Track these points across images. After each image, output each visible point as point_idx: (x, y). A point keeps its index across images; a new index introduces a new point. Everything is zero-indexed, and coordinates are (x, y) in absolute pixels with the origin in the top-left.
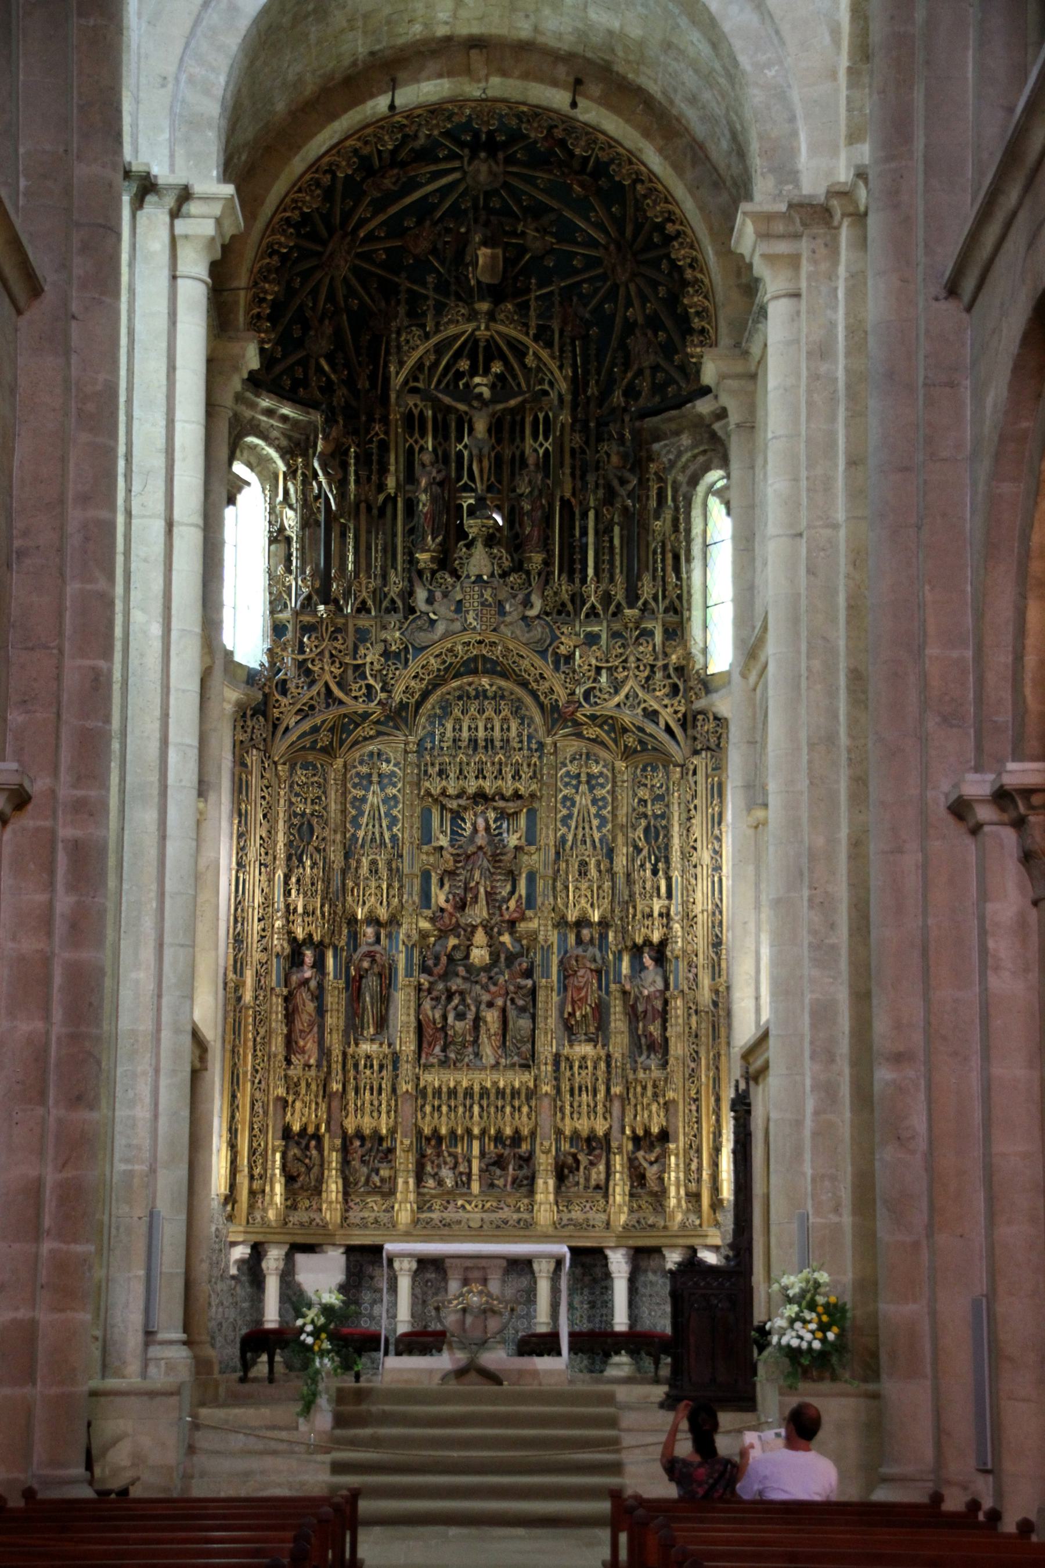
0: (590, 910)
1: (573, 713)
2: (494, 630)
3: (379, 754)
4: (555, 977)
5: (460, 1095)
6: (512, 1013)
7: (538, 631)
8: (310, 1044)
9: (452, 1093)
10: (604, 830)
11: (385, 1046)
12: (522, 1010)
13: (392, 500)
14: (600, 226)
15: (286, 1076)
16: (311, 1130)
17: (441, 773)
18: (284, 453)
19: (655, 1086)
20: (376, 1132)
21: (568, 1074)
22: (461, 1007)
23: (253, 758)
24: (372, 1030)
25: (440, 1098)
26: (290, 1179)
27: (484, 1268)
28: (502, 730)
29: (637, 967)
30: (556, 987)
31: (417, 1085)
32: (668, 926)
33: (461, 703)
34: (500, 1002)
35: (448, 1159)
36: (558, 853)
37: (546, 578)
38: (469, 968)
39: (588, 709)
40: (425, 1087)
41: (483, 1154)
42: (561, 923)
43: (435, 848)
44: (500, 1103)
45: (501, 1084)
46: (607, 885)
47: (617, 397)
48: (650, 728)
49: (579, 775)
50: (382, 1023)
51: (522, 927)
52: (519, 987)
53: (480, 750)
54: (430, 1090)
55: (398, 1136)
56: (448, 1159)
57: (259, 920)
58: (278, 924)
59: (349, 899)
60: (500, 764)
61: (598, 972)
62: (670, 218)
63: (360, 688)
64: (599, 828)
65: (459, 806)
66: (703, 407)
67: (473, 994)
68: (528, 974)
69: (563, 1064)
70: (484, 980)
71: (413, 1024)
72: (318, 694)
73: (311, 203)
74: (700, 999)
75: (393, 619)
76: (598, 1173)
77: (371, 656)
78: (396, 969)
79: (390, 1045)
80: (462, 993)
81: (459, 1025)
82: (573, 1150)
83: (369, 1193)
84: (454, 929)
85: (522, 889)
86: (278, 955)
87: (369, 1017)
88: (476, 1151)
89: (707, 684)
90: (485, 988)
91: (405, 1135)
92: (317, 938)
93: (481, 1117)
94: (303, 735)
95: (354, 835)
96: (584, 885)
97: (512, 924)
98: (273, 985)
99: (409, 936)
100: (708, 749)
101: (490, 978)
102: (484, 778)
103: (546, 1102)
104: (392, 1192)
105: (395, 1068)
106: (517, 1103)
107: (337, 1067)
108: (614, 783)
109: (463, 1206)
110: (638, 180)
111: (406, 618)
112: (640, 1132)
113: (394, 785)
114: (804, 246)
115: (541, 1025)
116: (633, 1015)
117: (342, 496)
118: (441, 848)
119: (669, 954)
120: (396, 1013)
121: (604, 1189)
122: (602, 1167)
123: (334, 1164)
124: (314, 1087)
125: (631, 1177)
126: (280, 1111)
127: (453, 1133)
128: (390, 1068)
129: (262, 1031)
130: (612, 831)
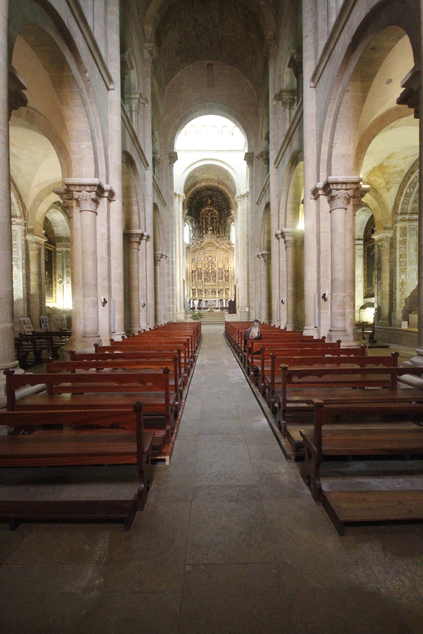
7: (215, 239)
8: (194, 281)
13: (201, 226)
14: (221, 198)
18: (190, 222)
23: (188, 252)
26: (193, 293)
29: (226, 272)
37: (216, 234)
39: (220, 247)
42: (218, 268)
47: (223, 215)
48: (227, 249)
50: (201, 278)
51: (214, 269)
62: (228, 197)
66: (232, 216)
68: (215, 273)
73: (192, 196)
75: (201, 238)
76: (222, 292)
77: (199, 242)
87: (200, 278)
89: (232, 245)
104: (202, 295)
110: (225, 193)
114: (242, 199)
116: (225, 277)
117: (196, 226)
121: (223, 294)
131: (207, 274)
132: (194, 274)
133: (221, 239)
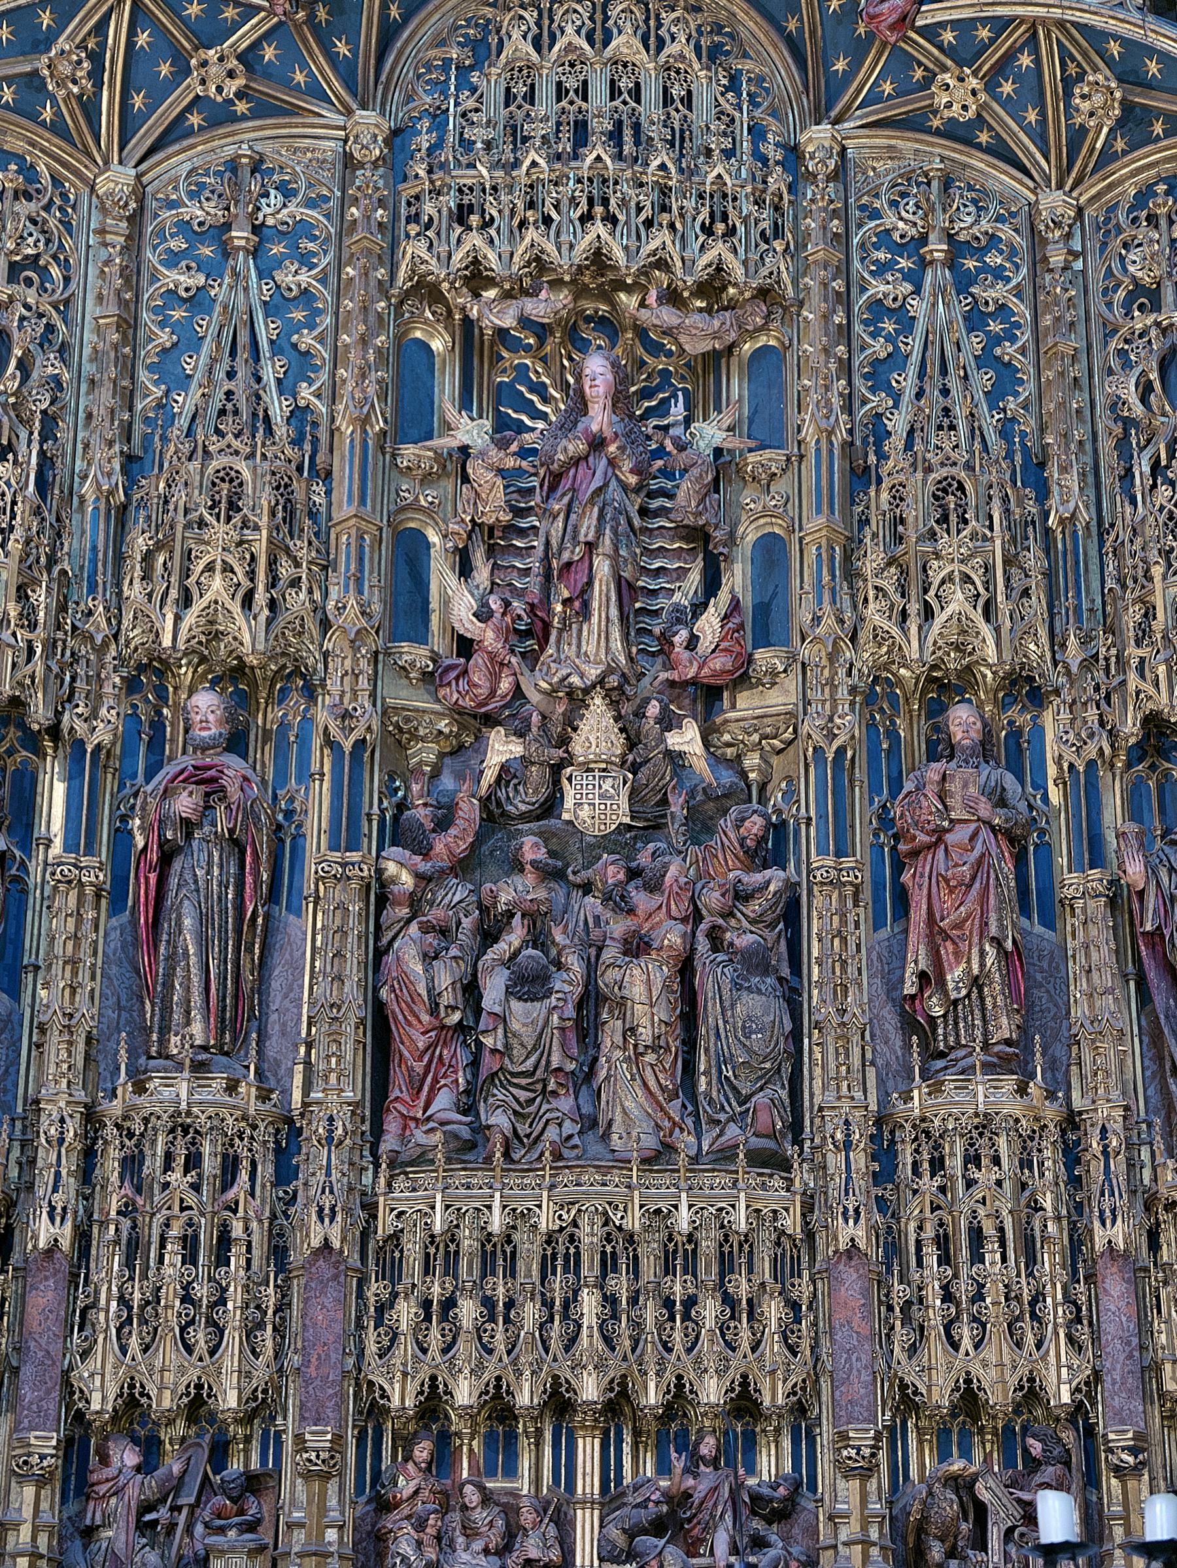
0: (986, 630)
1: (903, 21)
3: (256, 167)
5: (529, 1268)
17: (461, 215)
22: (530, 951)
25: (451, 1268)
28: (667, 100)
30: (866, 895)
34: (672, 936)
40: (395, 1237)
43: (440, 457)
45: (683, 1220)
49: (923, 239)
52: (742, 896)
56: (480, 1516)
59: (134, 591)
60: (665, 191)
64: (994, 397)
65: (525, 322)
70: (614, 874)
71: (355, 1006)
78: (298, 837)
88: (588, 1482)
90: (619, 902)
93: (607, 1340)
95: (160, 406)
101: (634, 874)
102: (611, 219)
105: (285, 1173)
106: (742, 1288)
108: (1039, 262)
113: (306, 261)
118: (464, 450)
120: (294, 985)
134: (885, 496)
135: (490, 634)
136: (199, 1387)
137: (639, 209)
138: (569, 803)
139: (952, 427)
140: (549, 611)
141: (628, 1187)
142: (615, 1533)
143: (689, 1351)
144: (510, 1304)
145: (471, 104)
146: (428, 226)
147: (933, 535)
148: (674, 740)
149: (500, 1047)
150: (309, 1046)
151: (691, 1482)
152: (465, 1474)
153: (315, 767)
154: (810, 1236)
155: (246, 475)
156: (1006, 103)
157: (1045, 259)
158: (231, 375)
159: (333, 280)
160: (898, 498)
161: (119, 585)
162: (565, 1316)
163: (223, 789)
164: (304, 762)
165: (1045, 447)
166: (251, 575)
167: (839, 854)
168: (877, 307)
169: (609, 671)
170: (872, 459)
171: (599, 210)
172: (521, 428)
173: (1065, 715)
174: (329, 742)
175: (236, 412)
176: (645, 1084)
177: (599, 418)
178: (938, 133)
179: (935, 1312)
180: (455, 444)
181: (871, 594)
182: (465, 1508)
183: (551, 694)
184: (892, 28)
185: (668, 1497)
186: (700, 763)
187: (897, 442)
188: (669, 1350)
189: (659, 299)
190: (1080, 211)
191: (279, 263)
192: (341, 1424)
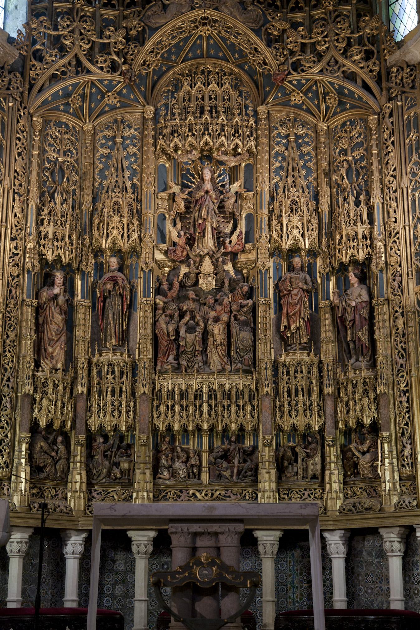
2: (216, 9)
4: (272, 296)
5: (191, 397)
6: (235, 327)
9: (184, 395)
10: (311, 179)
11: (126, 356)
12: (245, 324)
15: (33, 375)
16: (56, 426)
19: (365, 383)
20: (116, 429)
21: (286, 377)
22: (191, 322)
24: (113, 341)
25: (173, 398)
27: (216, 534)
28: (224, 100)
30: (272, 306)
31: (154, 389)
32: (372, 246)
33: (189, 78)
34: (225, 317)
35: (181, 454)
36: (272, 198)
38: (199, 293)
39: (295, 76)
40: (160, 390)
41: (211, 450)
44: (226, 403)
45: (227, 387)
46: (315, 221)
49: (288, 135)
51: (242, 258)
52: (242, 307)
53: (206, 113)
54: (164, 393)
55: (137, 433)
56: (181, 454)
57: (12, 239)
58: (30, 245)
59: (95, 233)
61: (308, 292)
63: (105, 61)
64: (306, 177)
67: (202, 313)
69: (280, 370)
70: (211, 301)
72: (69, 64)
74: (405, 302)
78: (136, 292)
79: (129, 357)
80: (192, 312)
81: (190, 337)
82: (291, 444)
83: (111, 484)
84: (186, 260)
85: (242, 226)
86: (29, 271)
88: (205, 447)
91: (142, 431)
92: (65, 260)
93: (210, 415)
94: (55, 96)
96: (296, 219)
97: (234, 256)
98: (25, 296)
99: (146, 263)
100: (404, 92)
101: (216, 301)
102: (209, 134)
103: (267, 401)
105: (134, 375)
106: (241, 403)
107: (82, 373)
109: (194, 494)
111: (143, 8)
112: (352, 424)
113: (134, 145)
115: (261, 336)
118: (174, 193)
119: (373, 267)
122: (318, 459)
123: (79, 457)
124: (61, 388)
125: (344, 466)
126: (27, 407)
127: (185, 430)
128: (130, 374)
129: (12, 335)
130: (316, 179)
131: (181, 298)
132: (56, 290)
133: (299, 17)
134: (278, 204)
135: (181, 241)
136: (116, 425)
137: (217, 131)
138: (200, 283)
139: (295, 186)
140: (195, 235)
141: (214, 379)
142: (211, 458)
143: (228, 417)
144: (187, 406)
145: (175, 102)
146: (164, 136)
147: (289, 215)
148: (226, 267)
149: (184, 345)
150: (139, 345)
151: (229, 447)
152: (177, 444)
153: (139, 275)
154: (257, 389)
155: (121, 203)
156: (310, 99)
157: (319, 140)
158: (117, 176)
159: (141, 150)
160: (280, 205)
161: (91, 231)
162: (200, 410)
163: (117, 282)
164: (137, 274)
165: (318, 190)
166: (123, 229)
167: (265, 297)
168: (277, 154)
169: (210, 251)
170: (275, 194)
171: (206, 132)
172: (189, 187)
173: (321, 260)
174: (142, 270)
175: (119, 187)
176: (218, 354)
177: (208, 186)
178: (293, 106)
179: (286, 408)
180: (172, 192)
181: (274, 230)
182: (177, 452)
183: (196, 256)
184: (280, 82)
185: (224, 450)
186: (232, 273)
187: (281, 190)
188: (224, 417)
189: (222, 153)
190: (328, 127)
191: (128, 146)
192: (149, 434)
